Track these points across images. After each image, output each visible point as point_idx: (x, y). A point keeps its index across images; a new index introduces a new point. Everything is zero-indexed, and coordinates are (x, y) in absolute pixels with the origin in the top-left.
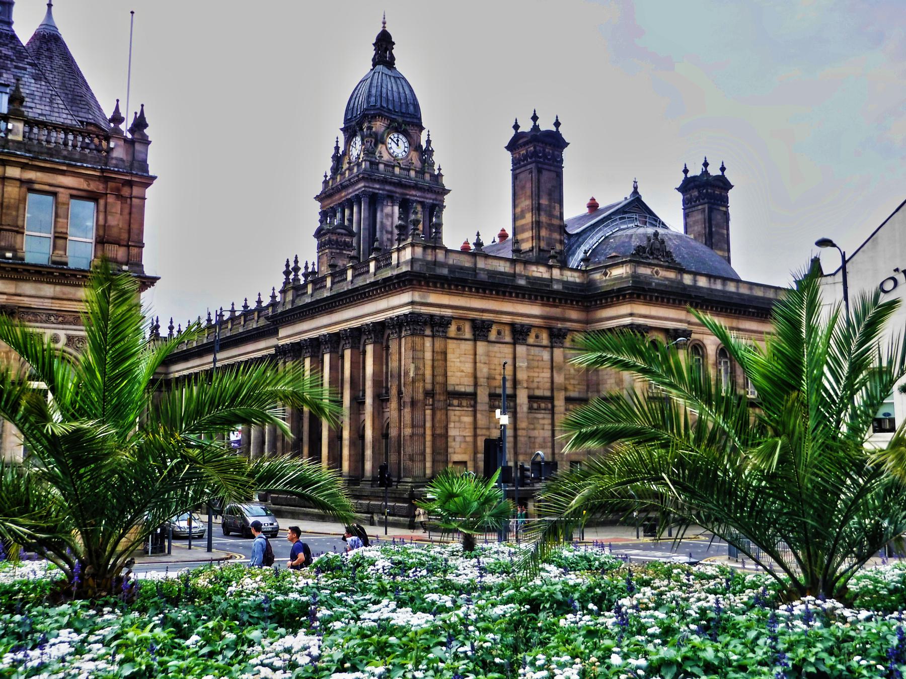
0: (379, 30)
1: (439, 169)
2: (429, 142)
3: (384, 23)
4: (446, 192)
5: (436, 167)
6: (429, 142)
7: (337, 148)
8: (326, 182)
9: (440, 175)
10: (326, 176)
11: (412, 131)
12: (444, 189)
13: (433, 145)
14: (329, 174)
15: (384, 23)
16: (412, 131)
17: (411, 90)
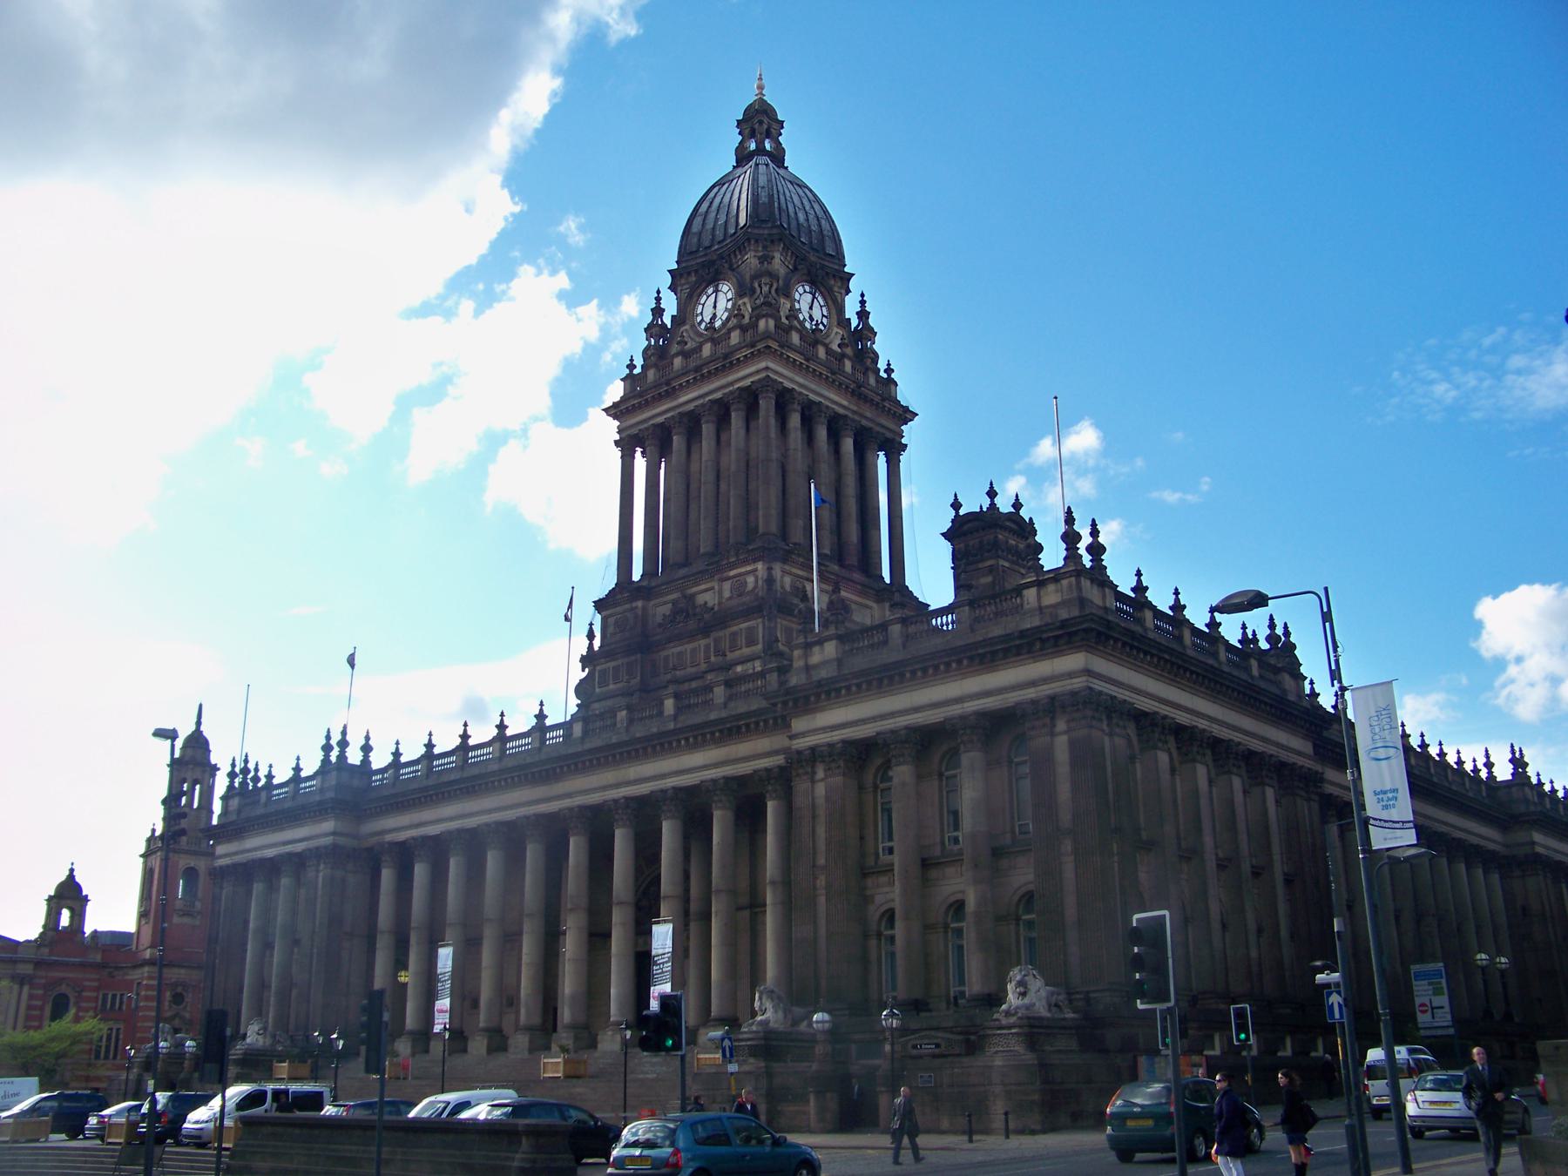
0: (751, 98)
1: (889, 370)
2: (863, 315)
3: (761, 88)
4: (907, 415)
5: (882, 365)
6: (863, 315)
7: (658, 311)
8: (629, 379)
9: (891, 382)
10: (631, 366)
11: (836, 286)
12: (906, 409)
13: (871, 321)
14: (639, 362)
15: (761, 88)
16: (836, 286)
17: (826, 211)
